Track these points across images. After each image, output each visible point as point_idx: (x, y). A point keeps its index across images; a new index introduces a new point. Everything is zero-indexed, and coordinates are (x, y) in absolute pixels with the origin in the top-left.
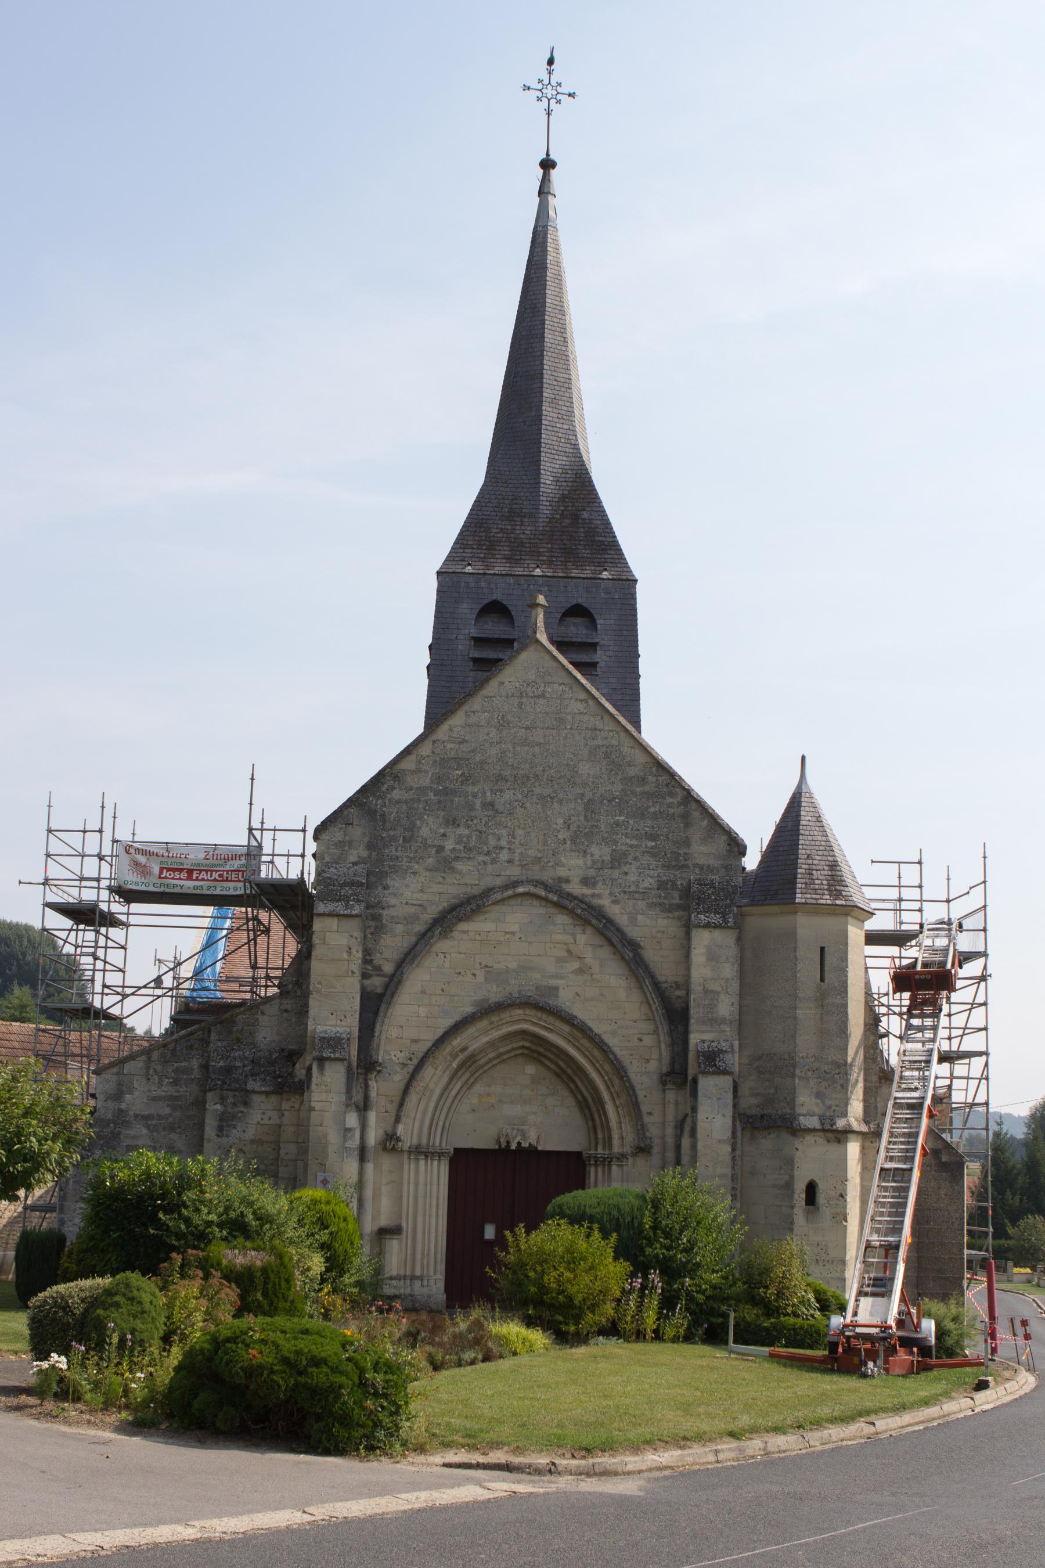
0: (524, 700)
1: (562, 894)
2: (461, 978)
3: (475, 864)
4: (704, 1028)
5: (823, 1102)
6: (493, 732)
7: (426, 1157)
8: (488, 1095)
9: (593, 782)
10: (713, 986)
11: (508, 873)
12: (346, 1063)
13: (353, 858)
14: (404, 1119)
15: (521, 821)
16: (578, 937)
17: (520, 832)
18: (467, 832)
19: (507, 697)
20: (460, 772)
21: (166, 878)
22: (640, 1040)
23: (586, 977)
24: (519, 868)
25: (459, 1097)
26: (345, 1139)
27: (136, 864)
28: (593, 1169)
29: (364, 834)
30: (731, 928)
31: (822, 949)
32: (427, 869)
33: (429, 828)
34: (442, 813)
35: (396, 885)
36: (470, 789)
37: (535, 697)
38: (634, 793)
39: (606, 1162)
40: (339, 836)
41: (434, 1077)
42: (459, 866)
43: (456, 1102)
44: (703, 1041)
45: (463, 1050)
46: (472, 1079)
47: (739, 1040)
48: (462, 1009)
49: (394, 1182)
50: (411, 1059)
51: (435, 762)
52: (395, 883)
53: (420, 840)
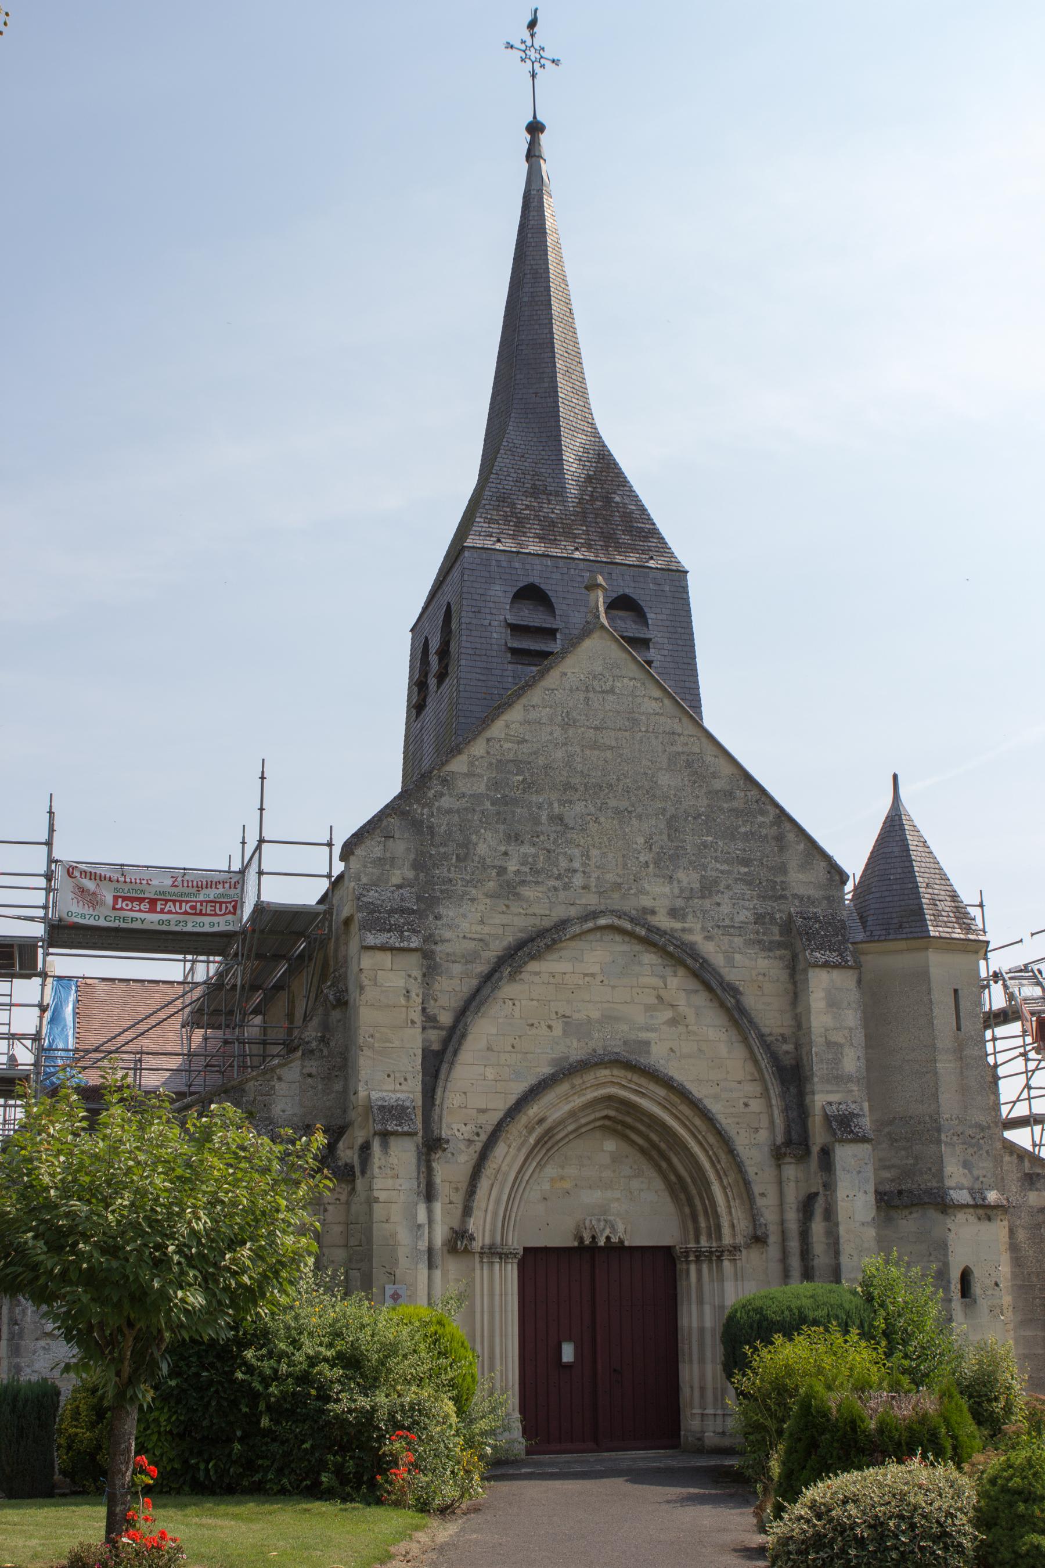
0: (591, 695)
1: (651, 929)
2: (534, 1031)
3: (544, 889)
4: (829, 1088)
5: (970, 1172)
6: (558, 732)
8: (562, 1178)
9: (675, 796)
10: (837, 1037)
11: (584, 901)
13: (396, 880)
15: (596, 838)
16: (669, 980)
17: (594, 852)
18: (532, 850)
19: (571, 690)
20: (520, 778)
21: (122, 909)
22: (746, 1105)
23: (681, 1029)
24: (597, 896)
26: (418, 1238)
27: (83, 890)
28: (693, 1268)
29: (408, 849)
30: (850, 967)
31: (956, 991)
32: (487, 895)
33: (487, 844)
34: (502, 827)
35: (451, 914)
36: (534, 798)
37: (603, 692)
38: (721, 809)
39: (716, 1256)
40: (377, 852)
41: (507, 1156)
42: (526, 892)
44: (830, 1104)
45: (541, 1121)
47: (869, 1101)
48: (538, 1070)
50: (478, 1134)
51: (491, 764)
52: (448, 911)
53: (477, 859)
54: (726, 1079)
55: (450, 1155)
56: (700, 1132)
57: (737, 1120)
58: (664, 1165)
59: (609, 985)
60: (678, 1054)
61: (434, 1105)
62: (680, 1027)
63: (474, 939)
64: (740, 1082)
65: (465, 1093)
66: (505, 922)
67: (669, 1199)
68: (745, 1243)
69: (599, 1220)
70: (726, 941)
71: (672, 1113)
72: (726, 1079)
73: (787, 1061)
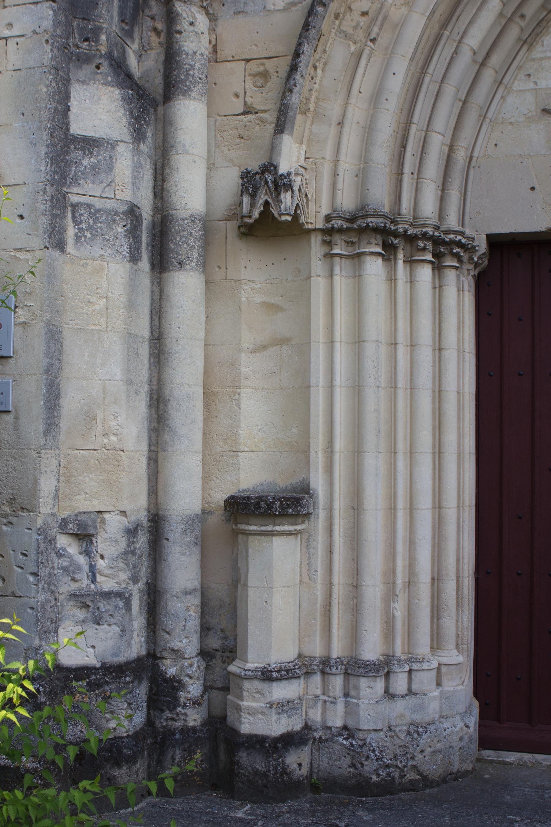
7: (388, 252)
25: (496, 60)
43: (488, 76)
49: (281, 341)
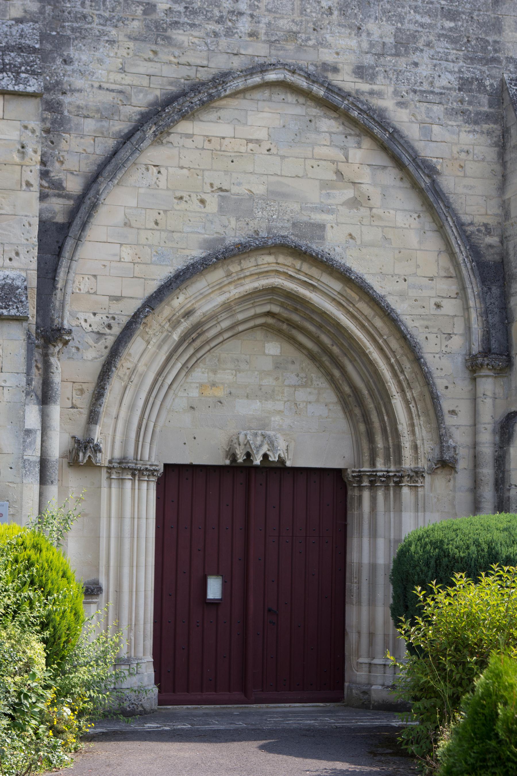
1: (330, 88)
2: (183, 205)
3: (202, 34)
8: (214, 385)
12: (25, 324)
14: (103, 419)
16: (352, 152)
22: (438, 306)
23: (364, 211)
24: (267, 46)
26: (25, 446)
28: (366, 495)
32: (130, 38)
35: (84, 58)
39: (395, 481)
41: (144, 354)
42: (179, 36)
45: (188, 314)
46: (194, 359)
48: (187, 252)
49: (85, 515)
50: (109, 327)
52: (81, 54)
54: (415, 274)
55: (74, 350)
56: (381, 336)
57: (426, 323)
58: (337, 373)
59: (277, 155)
60: (359, 242)
61: (54, 288)
62: (362, 209)
63: (113, 91)
64: (431, 279)
65: (95, 276)
66: (150, 71)
67: (340, 414)
68: (430, 468)
69: (256, 435)
70: (423, 109)
71: (348, 312)
72: (415, 274)
73: (490, 256)
